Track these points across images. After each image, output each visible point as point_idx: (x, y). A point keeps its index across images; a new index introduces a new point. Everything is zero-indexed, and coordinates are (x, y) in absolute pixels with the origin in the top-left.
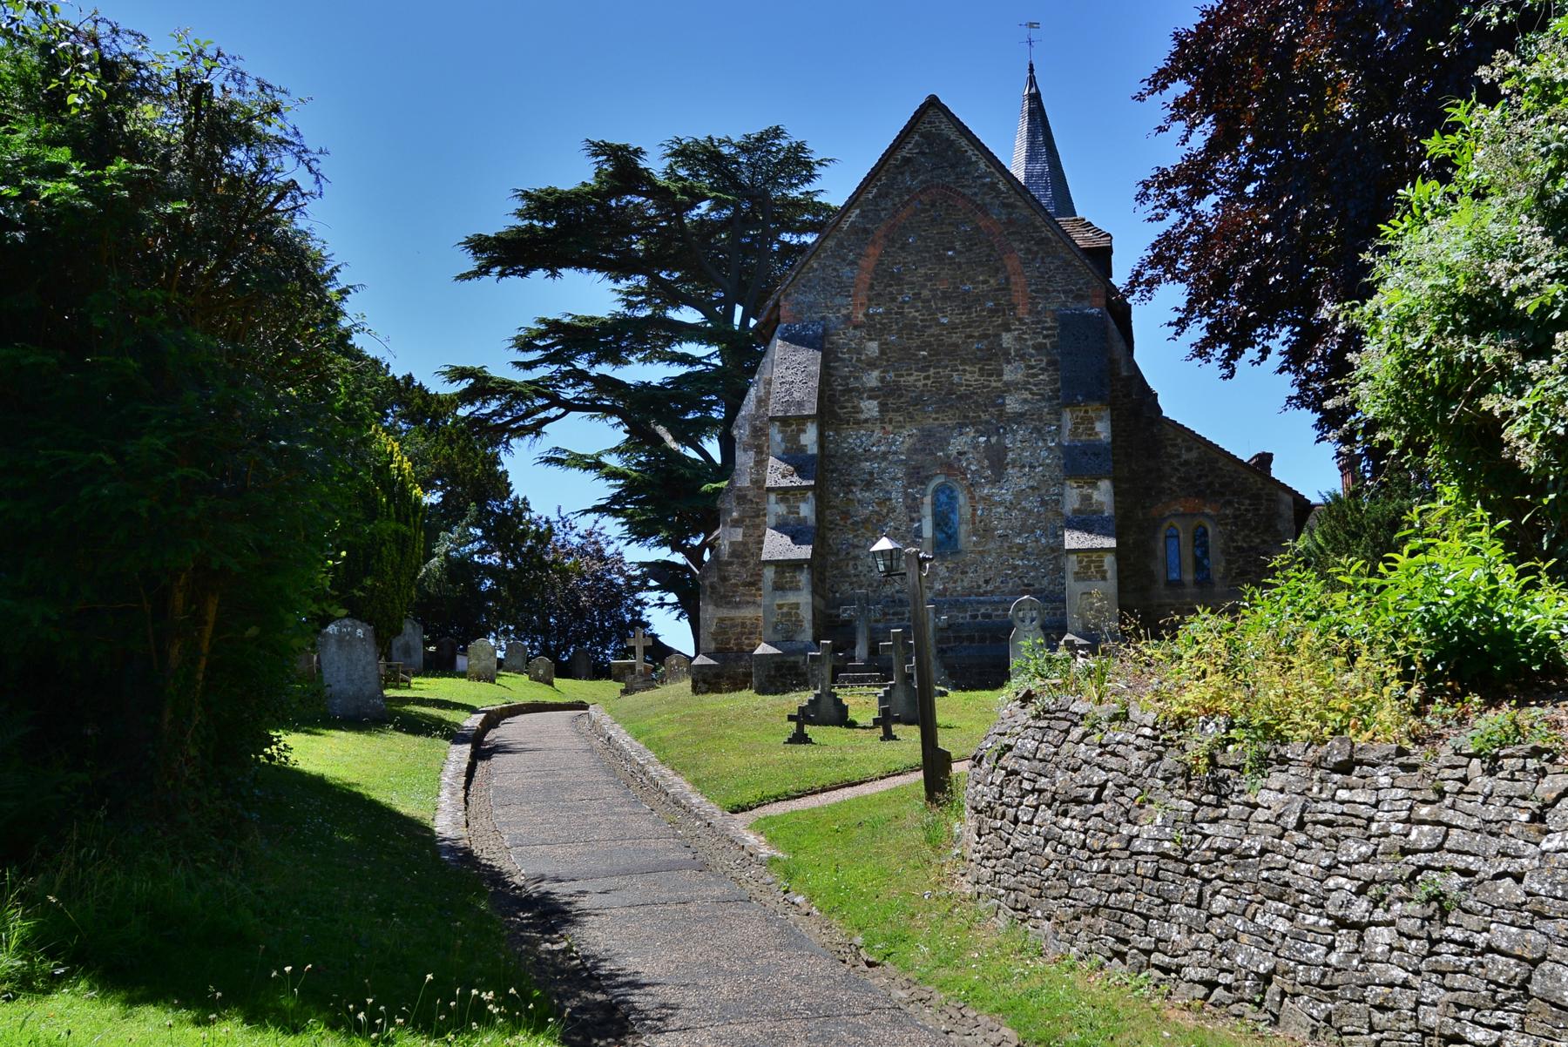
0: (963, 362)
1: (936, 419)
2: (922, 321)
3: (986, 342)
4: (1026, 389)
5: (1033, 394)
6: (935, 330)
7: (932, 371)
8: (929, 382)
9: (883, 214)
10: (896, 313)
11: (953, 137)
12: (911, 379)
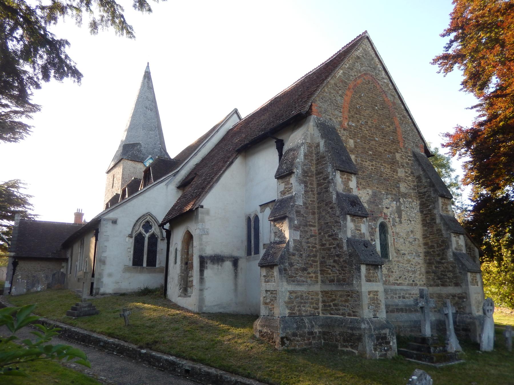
0: (385, 162)
1: (377, 188)
2: (369, 136)
3: (391, 155)
4: (406, 182)
5: (408, 185)
6: (373, 142)
7: (374, 163)
8: (373, 168)
9: (351, 77)
10: (360, 129)
11: (373, 56)
12: (367, 164)
